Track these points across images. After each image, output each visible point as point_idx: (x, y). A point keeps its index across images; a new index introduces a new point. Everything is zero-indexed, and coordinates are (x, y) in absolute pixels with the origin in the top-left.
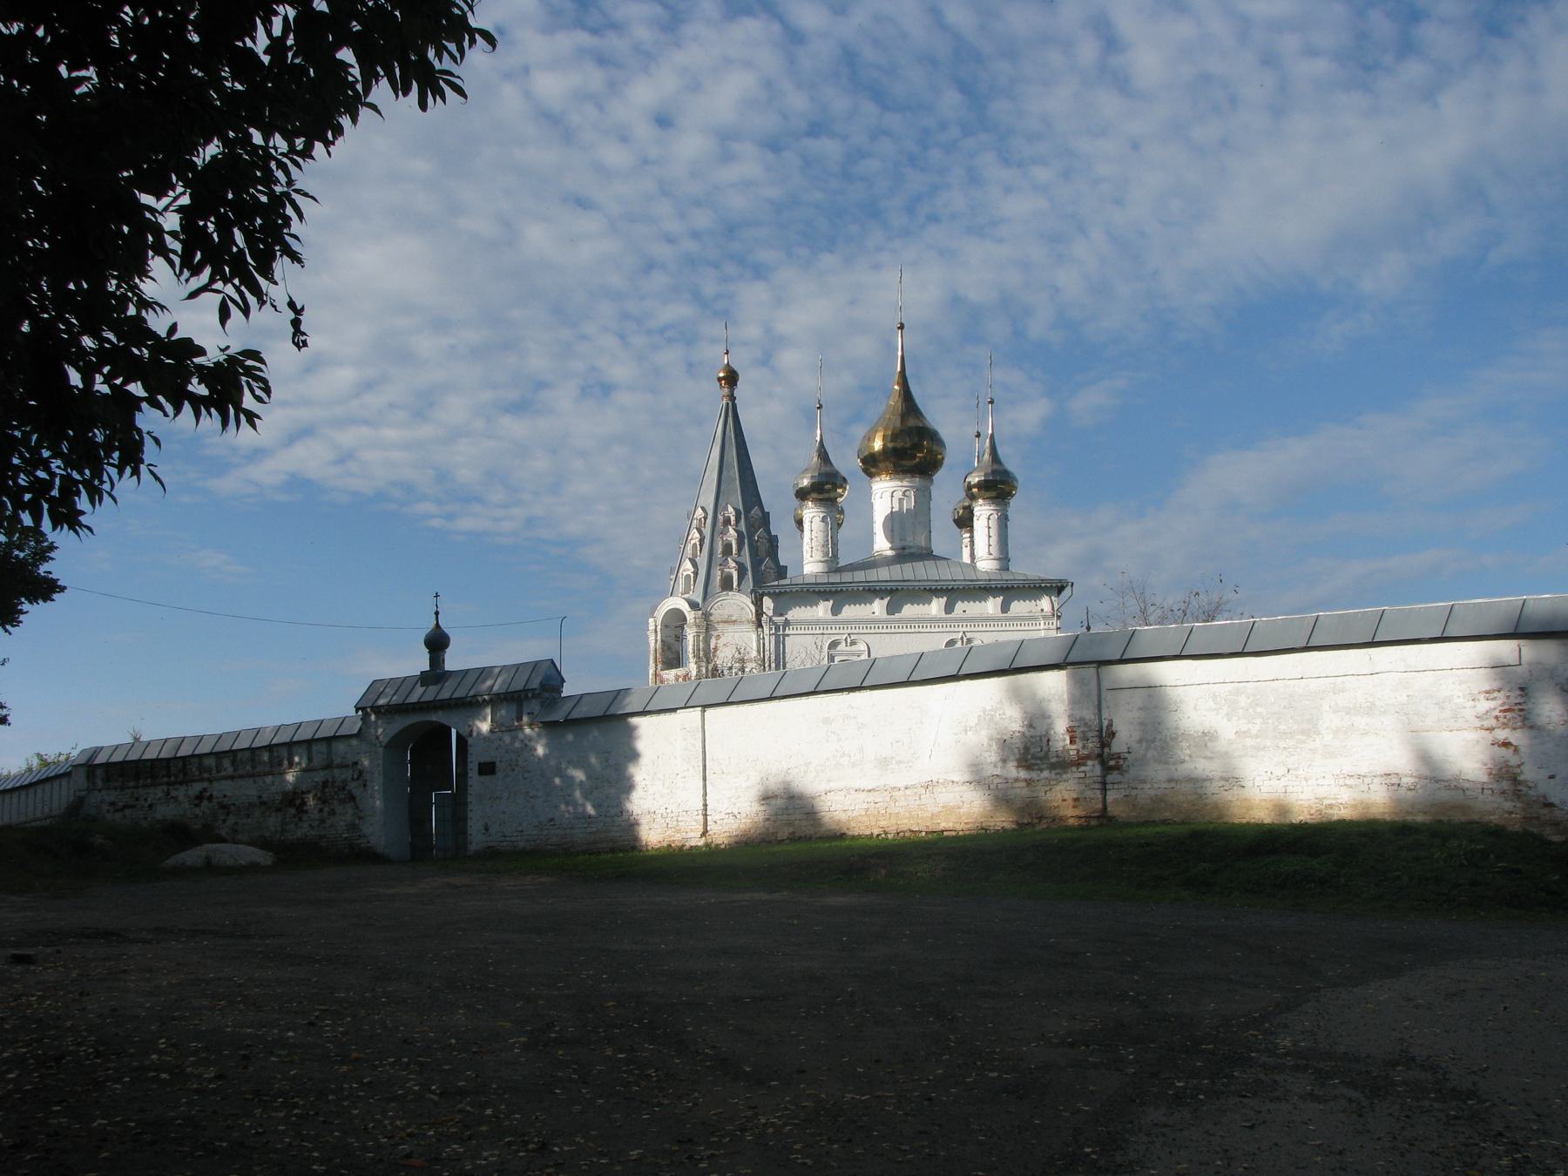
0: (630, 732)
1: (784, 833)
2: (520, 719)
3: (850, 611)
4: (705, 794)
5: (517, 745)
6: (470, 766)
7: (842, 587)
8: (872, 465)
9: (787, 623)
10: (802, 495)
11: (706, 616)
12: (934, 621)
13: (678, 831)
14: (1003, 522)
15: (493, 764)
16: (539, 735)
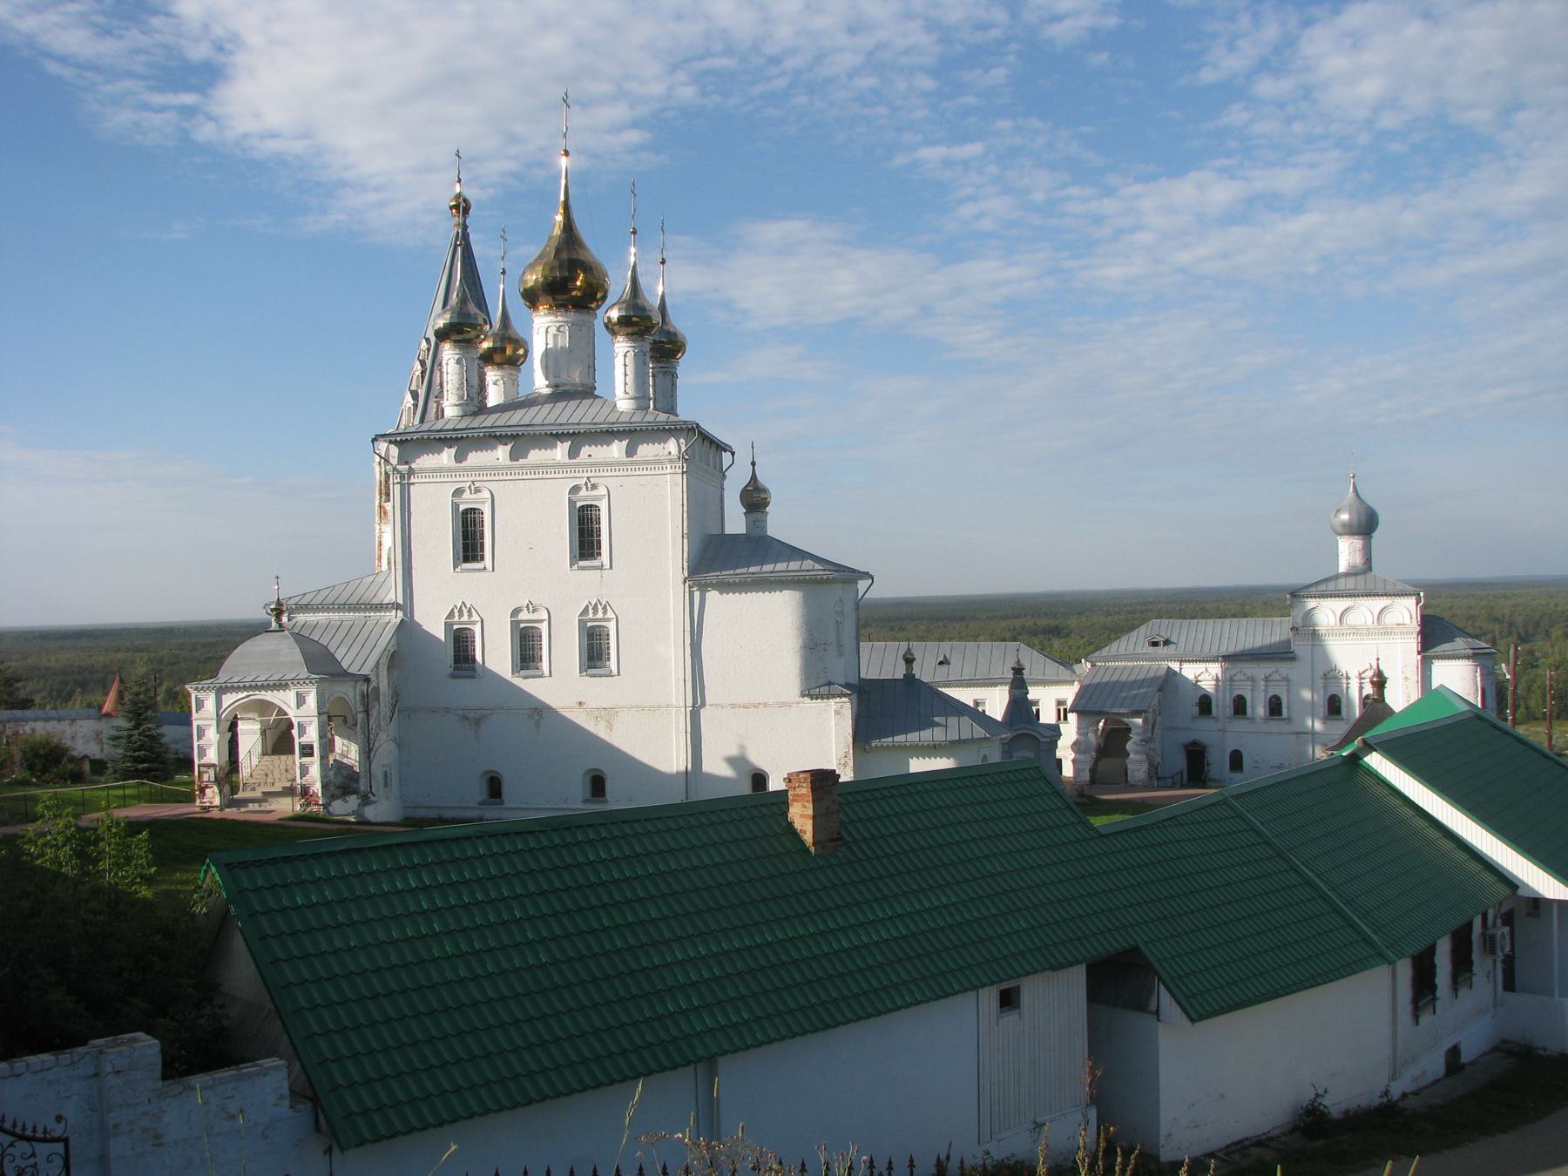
3: (475, 458)
9: (411, 472)
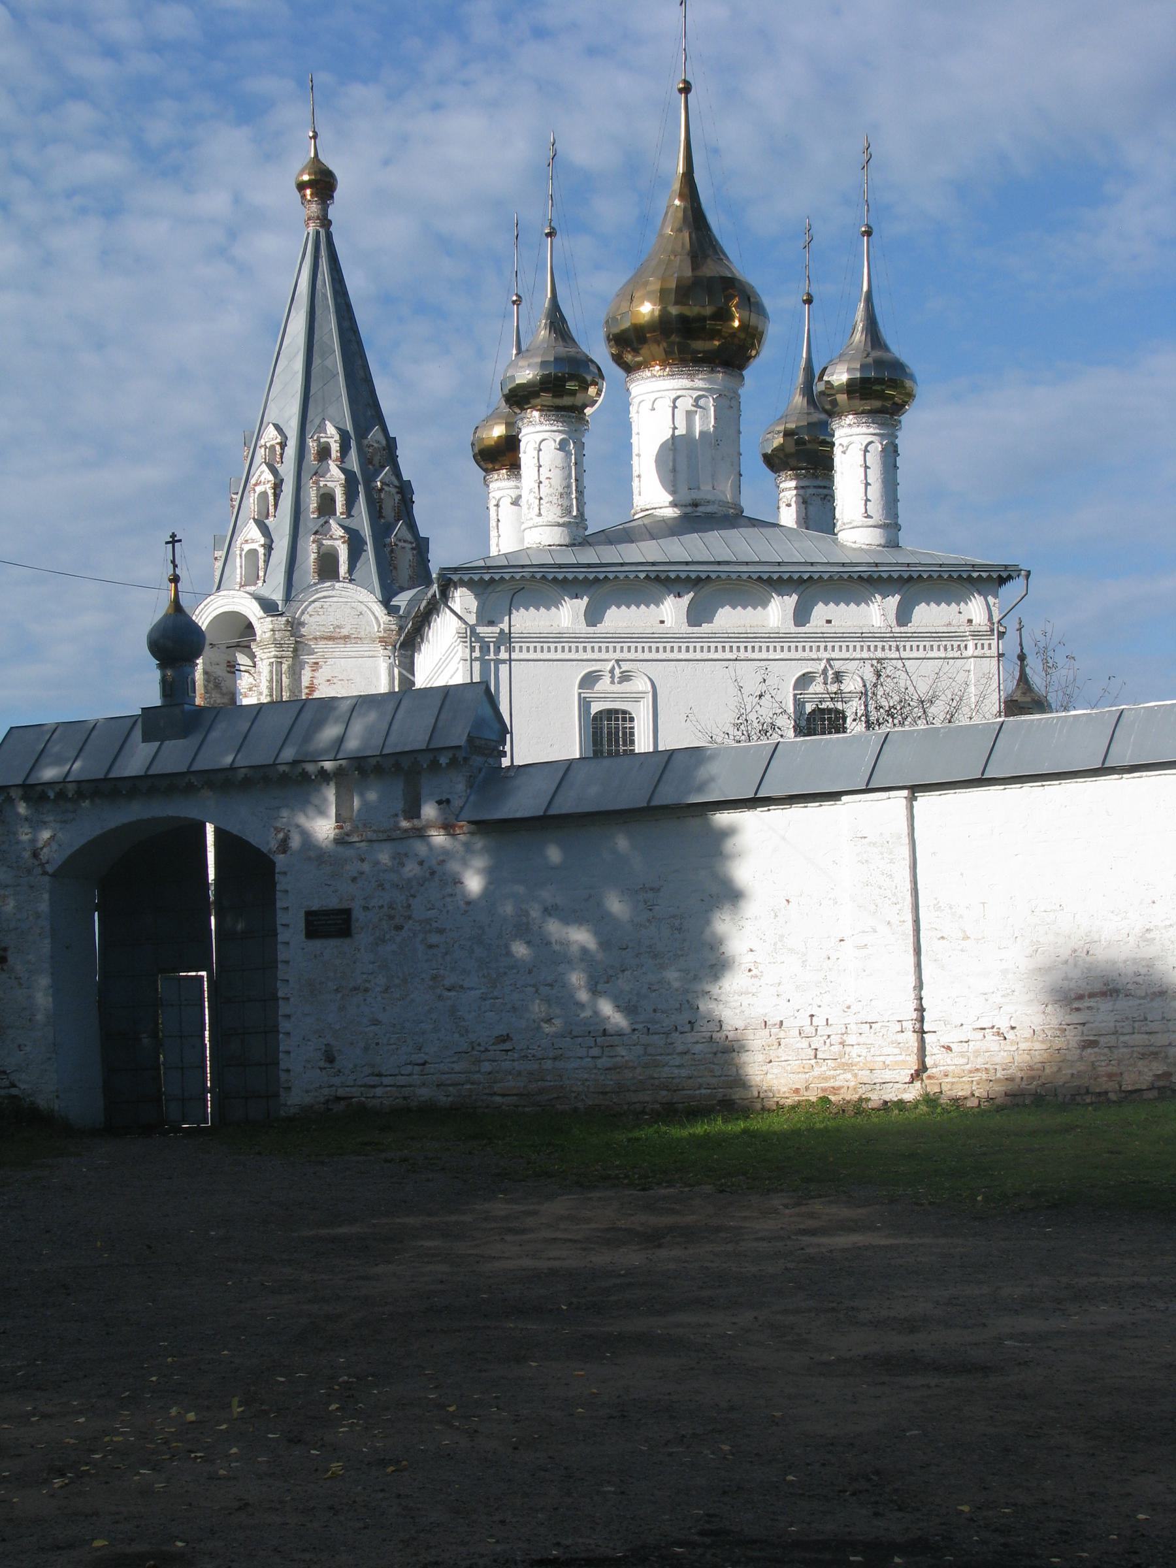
0: (716, 844)
1: (1140, 1075)
2: (413, 812)
3: (618, 618)
4: (919, 986)
5: (411, 869)
6: (282, 918)
7: (592, 570)
8: (631, 346)
10: (519, 398)
11: (294, 626)
12: (776, 638)
13: (847, 1067)
14: (891, 454)
15: (347, 912)
16: (467, 846)
